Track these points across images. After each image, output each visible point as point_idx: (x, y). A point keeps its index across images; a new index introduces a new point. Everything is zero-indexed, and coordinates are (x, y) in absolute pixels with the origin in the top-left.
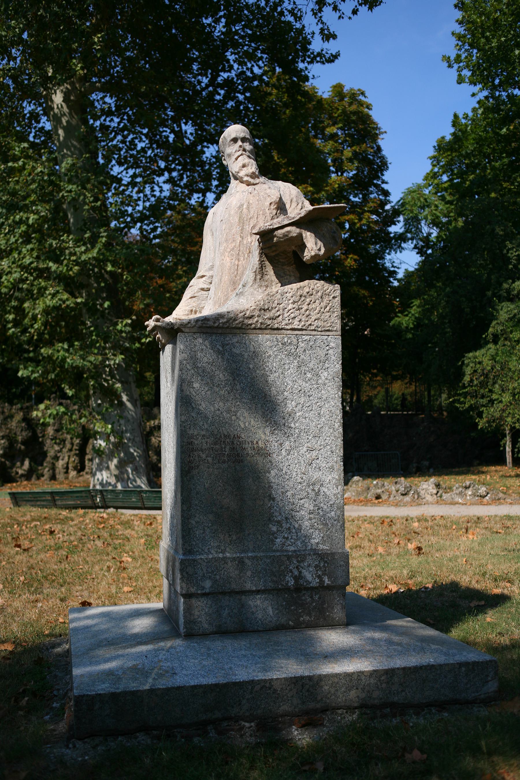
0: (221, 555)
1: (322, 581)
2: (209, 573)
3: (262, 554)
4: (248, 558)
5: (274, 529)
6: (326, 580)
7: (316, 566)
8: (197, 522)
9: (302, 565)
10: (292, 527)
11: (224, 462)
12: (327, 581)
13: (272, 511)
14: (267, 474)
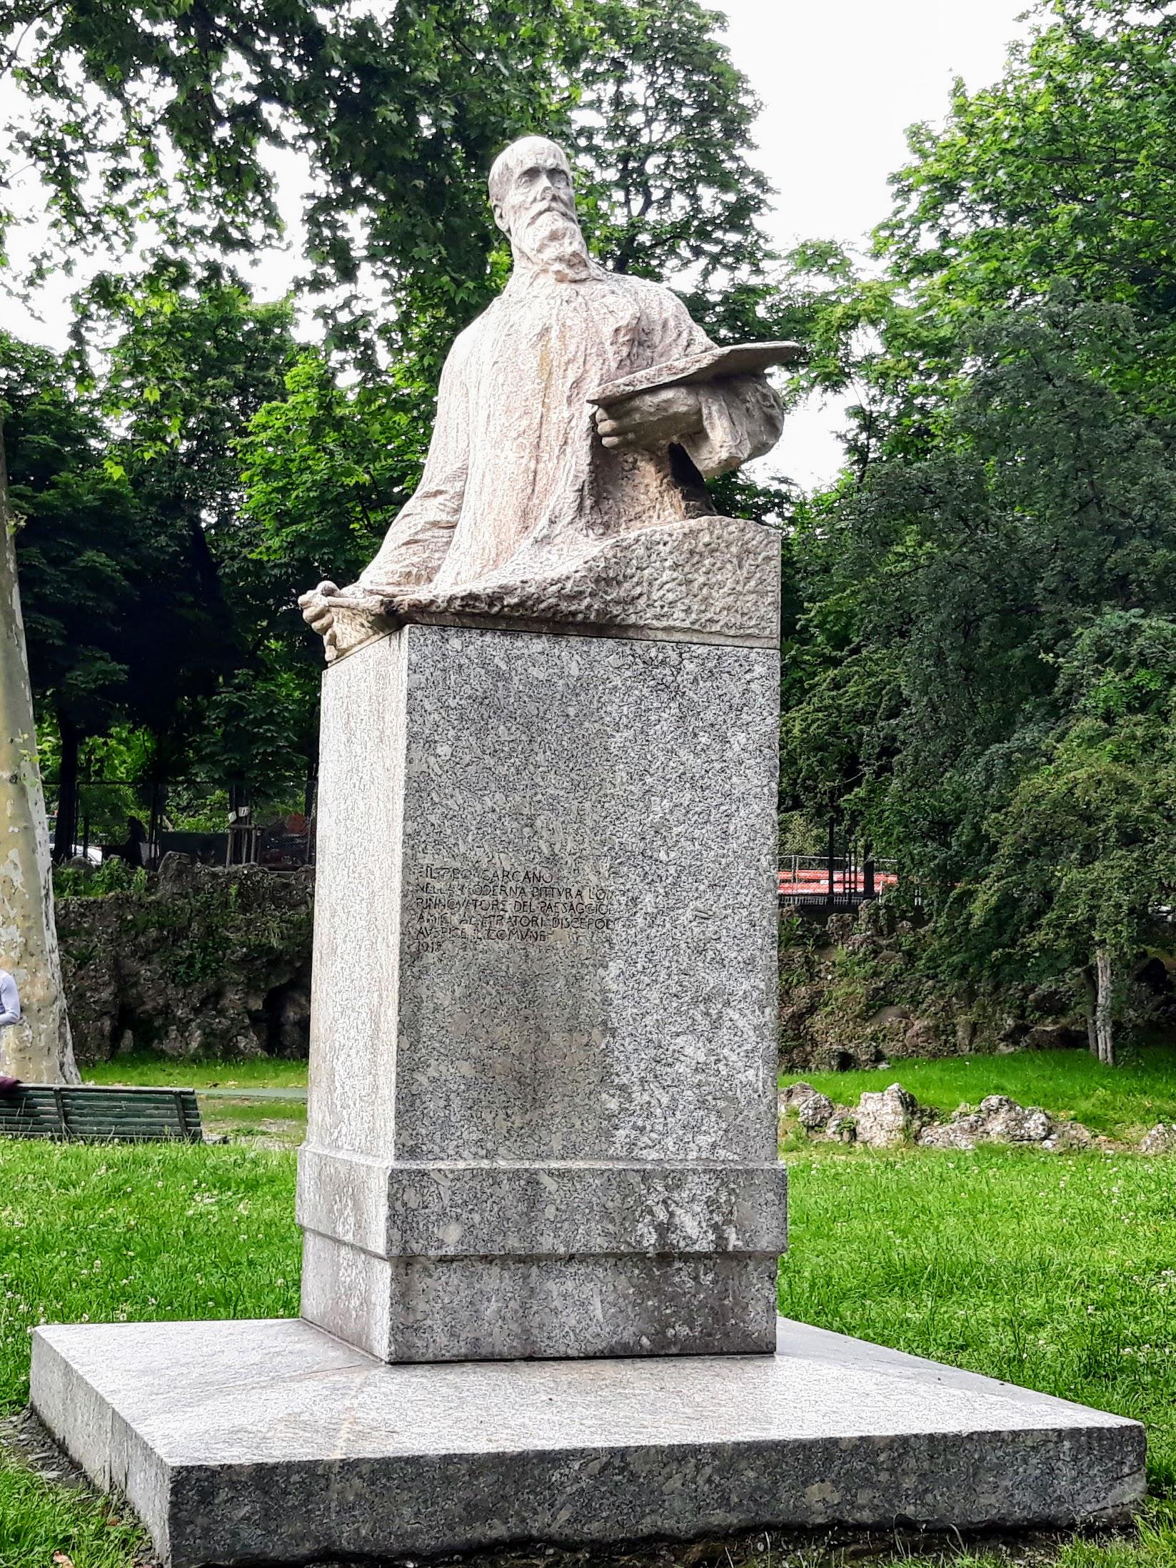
0: (485, 1164)
1: (721, 1238)
2: (457, 1206)
3: (581, 1165)
4: (550, 1173)
5: (613, 1105)
6: (733, 1237)
7: (710, 1202)
8: (433, 1080)
9: (676, 1196)
10: (654, 1102)
11: (501, 936)
12: (733, 1240)
13: (608, 1060)
14: (601, 971)
